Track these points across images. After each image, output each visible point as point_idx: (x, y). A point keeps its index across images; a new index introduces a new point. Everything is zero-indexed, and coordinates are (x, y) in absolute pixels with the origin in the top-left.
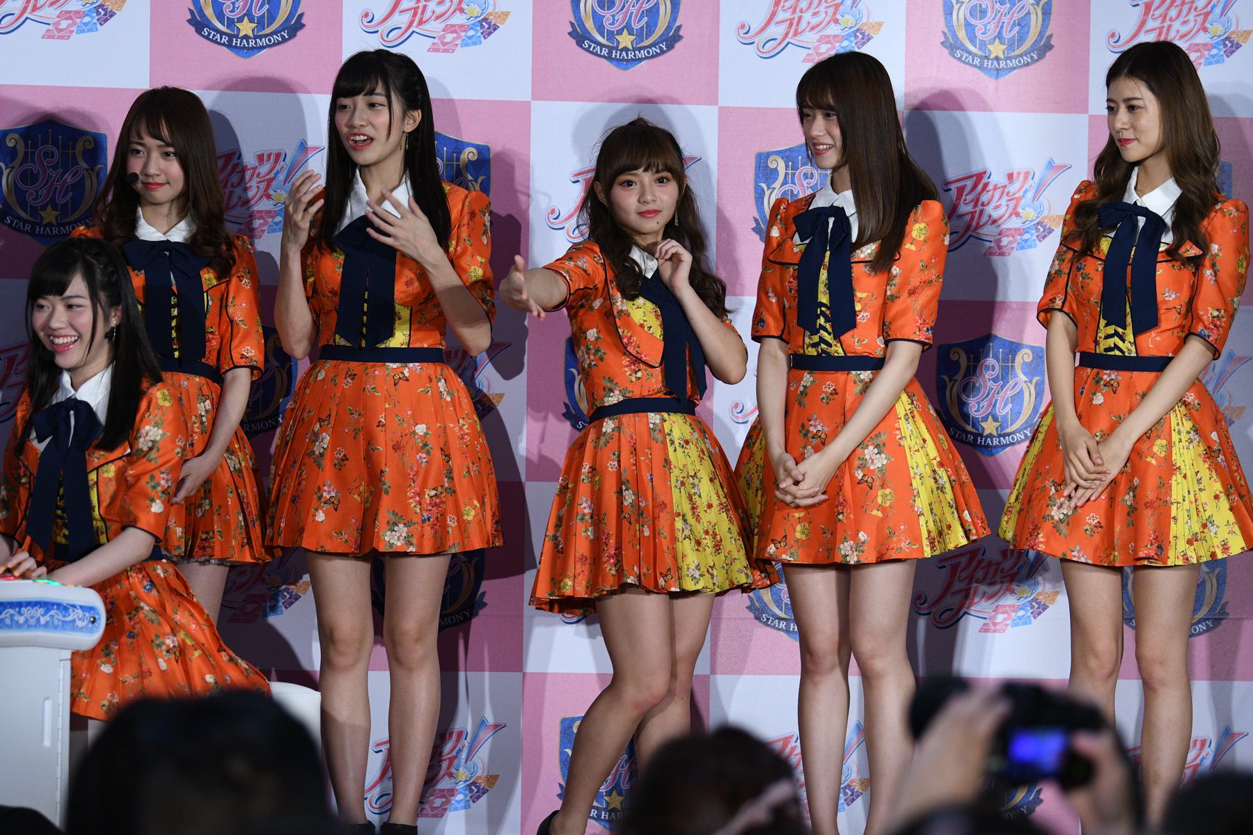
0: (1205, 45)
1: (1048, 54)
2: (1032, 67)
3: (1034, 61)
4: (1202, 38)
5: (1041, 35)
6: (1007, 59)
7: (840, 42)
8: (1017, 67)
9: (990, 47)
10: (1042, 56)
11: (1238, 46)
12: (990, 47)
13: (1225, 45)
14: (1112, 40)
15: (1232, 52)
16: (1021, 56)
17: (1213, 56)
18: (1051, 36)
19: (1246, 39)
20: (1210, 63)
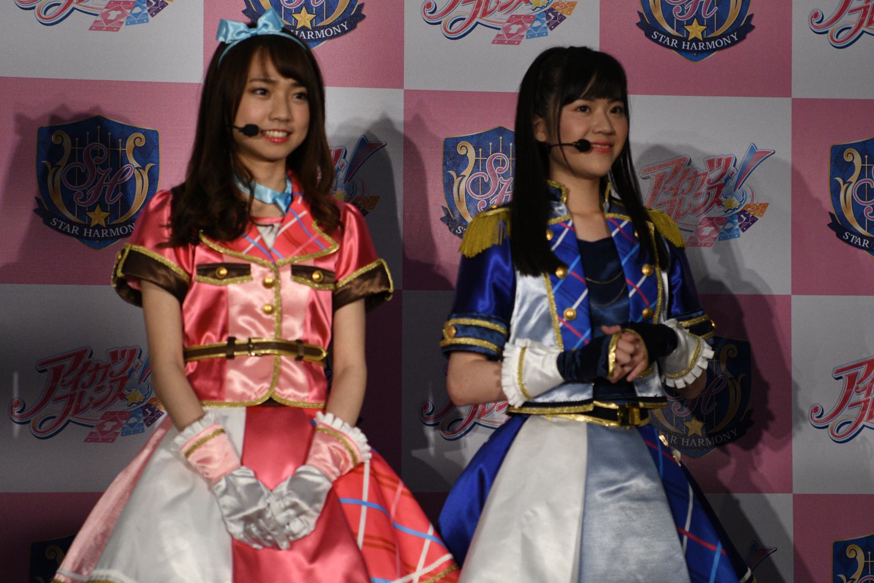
0: (527, 17)
1: (359, 25)
2: (342, 38)
3: (344, 32)
4: (524, 10)
5: (351, 6)
6: (314, 29)
7: (132, 8)
8: (326, 38)
9: (296, 16)
10: (352, 26)
11: (562, 18)
12: (296, 16)
13: (548, 17)
14: (427, 11)
15: (556, 25)
16: (330, 26)
17: (536, 29)
18: (361, 6)
19: (571, 10)
20: (533, 36)
